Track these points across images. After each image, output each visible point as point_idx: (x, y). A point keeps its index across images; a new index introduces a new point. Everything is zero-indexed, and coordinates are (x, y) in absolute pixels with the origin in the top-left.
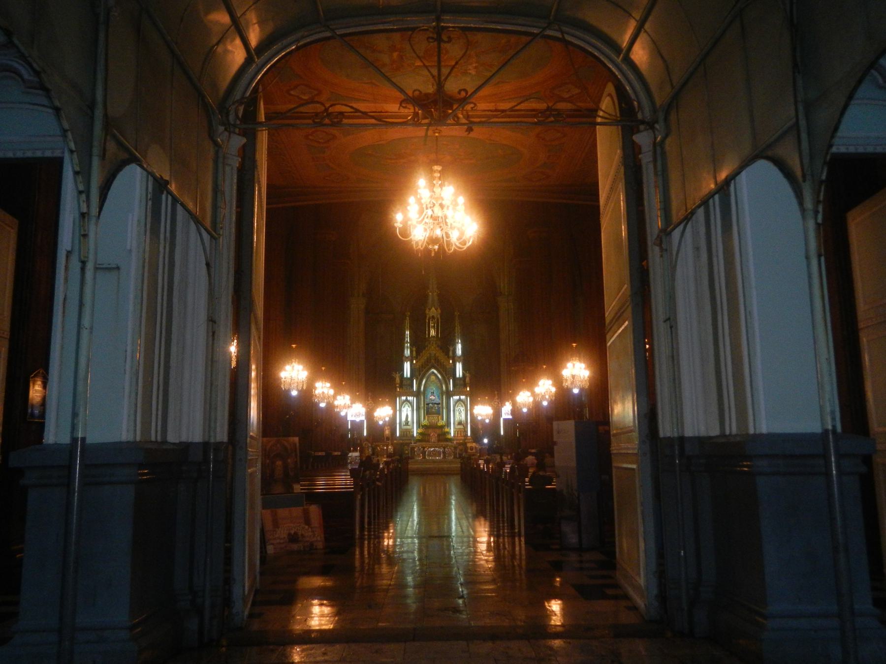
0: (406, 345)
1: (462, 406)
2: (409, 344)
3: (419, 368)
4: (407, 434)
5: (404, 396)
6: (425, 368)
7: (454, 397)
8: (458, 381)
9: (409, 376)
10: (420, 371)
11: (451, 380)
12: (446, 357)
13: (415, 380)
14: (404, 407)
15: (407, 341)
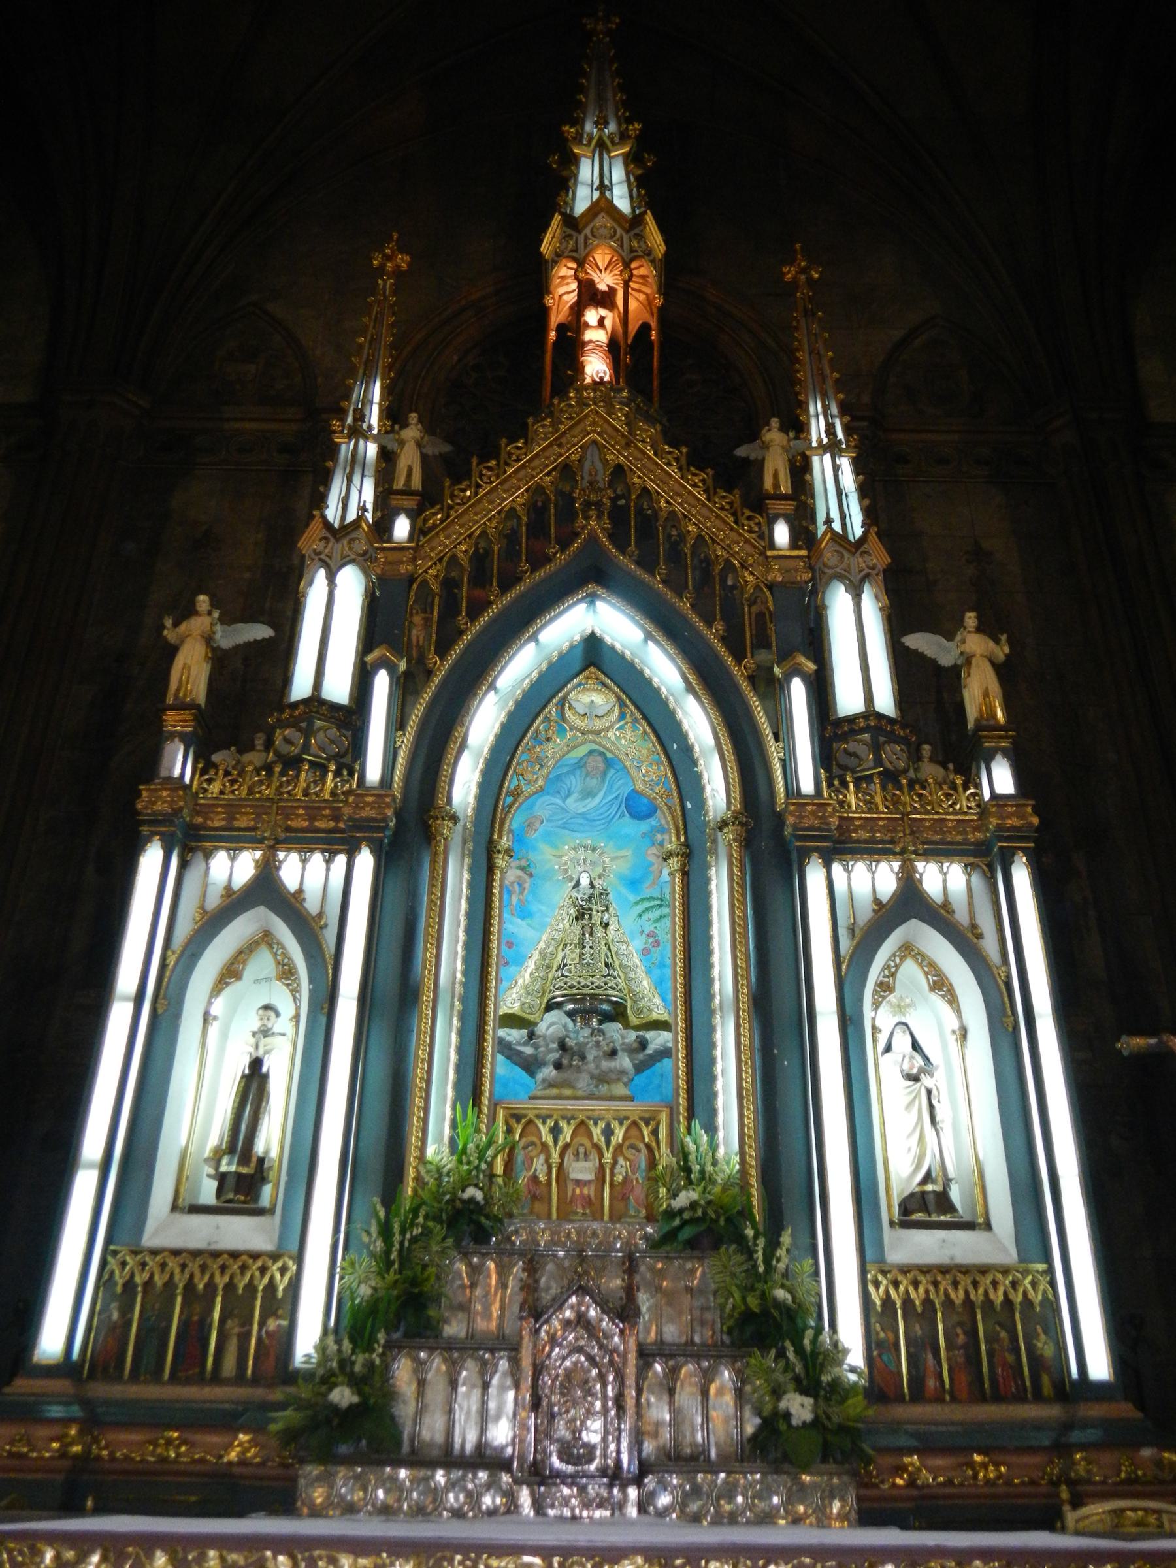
0: (346, 449)
1: (941, 984)
2: (372, 450)
3: (450, 585)
4: (195, 1333)
5: (236, 841)
6: (505, 588)
7: (837, 868)
8: (860, 746)
9: (338, 689)
10: (450, 609)
11: (798, 691)
12: (736, 497)
13: (382, 682)
14: (230, 973)
15: (360, 416)
